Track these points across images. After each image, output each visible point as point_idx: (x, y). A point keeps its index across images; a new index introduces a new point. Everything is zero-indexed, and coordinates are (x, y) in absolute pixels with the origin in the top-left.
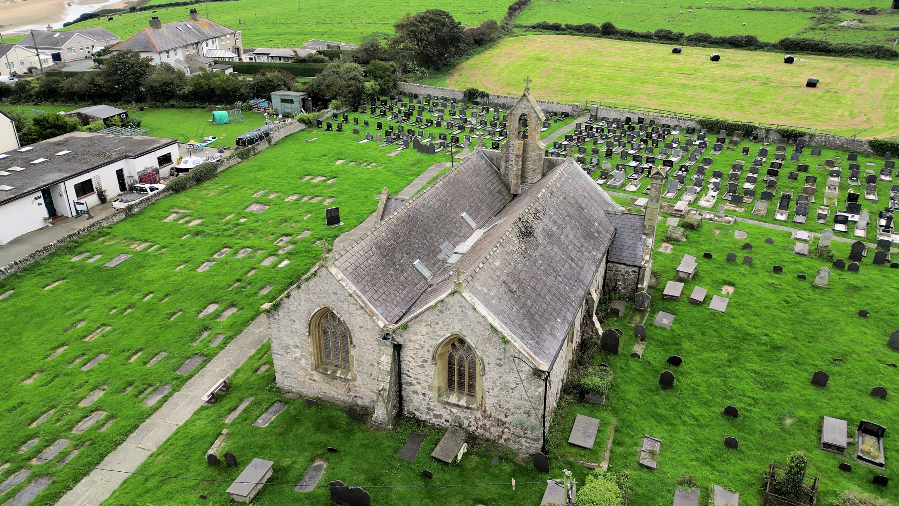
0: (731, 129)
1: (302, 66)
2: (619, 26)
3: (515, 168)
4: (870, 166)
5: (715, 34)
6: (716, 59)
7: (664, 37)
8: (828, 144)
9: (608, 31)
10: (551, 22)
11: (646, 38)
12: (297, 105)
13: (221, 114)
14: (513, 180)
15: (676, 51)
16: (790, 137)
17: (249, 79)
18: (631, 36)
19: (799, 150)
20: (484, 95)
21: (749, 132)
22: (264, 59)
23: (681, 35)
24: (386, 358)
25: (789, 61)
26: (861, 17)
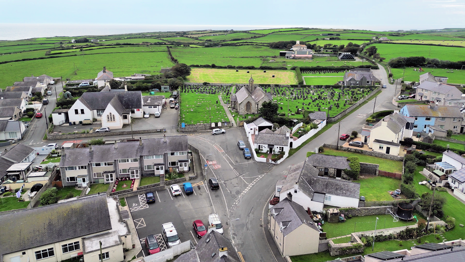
0: (266, 85)
1: (148, 81)
2: (216, 65)
3: (250, 89)
4: (292, 89)
5: (244, 66)
6: (248, 72)
7: (230, 67)
8: (283, 86)
9: (214, 66)
10: (195, 64)
11: (225, 68)
12: (168, 89)
13: (152, 92)
14: (250, 91)
15: (237, 71)
16: (277, 86)
17: (150, 84)
18: (221, 67)
19: (279, 87)
20: (208, 83)
21: (269, 86)
22: (129, 80)
23: (235, 67)
24: (257, 106)
25: (265, 72)
26: (273, 59)
